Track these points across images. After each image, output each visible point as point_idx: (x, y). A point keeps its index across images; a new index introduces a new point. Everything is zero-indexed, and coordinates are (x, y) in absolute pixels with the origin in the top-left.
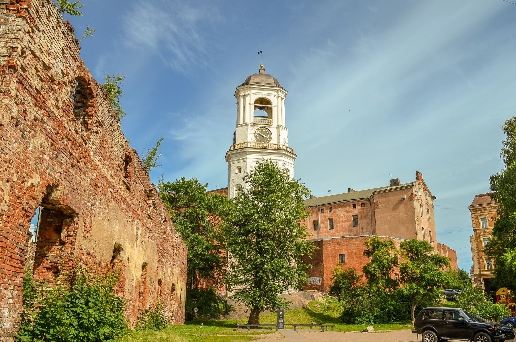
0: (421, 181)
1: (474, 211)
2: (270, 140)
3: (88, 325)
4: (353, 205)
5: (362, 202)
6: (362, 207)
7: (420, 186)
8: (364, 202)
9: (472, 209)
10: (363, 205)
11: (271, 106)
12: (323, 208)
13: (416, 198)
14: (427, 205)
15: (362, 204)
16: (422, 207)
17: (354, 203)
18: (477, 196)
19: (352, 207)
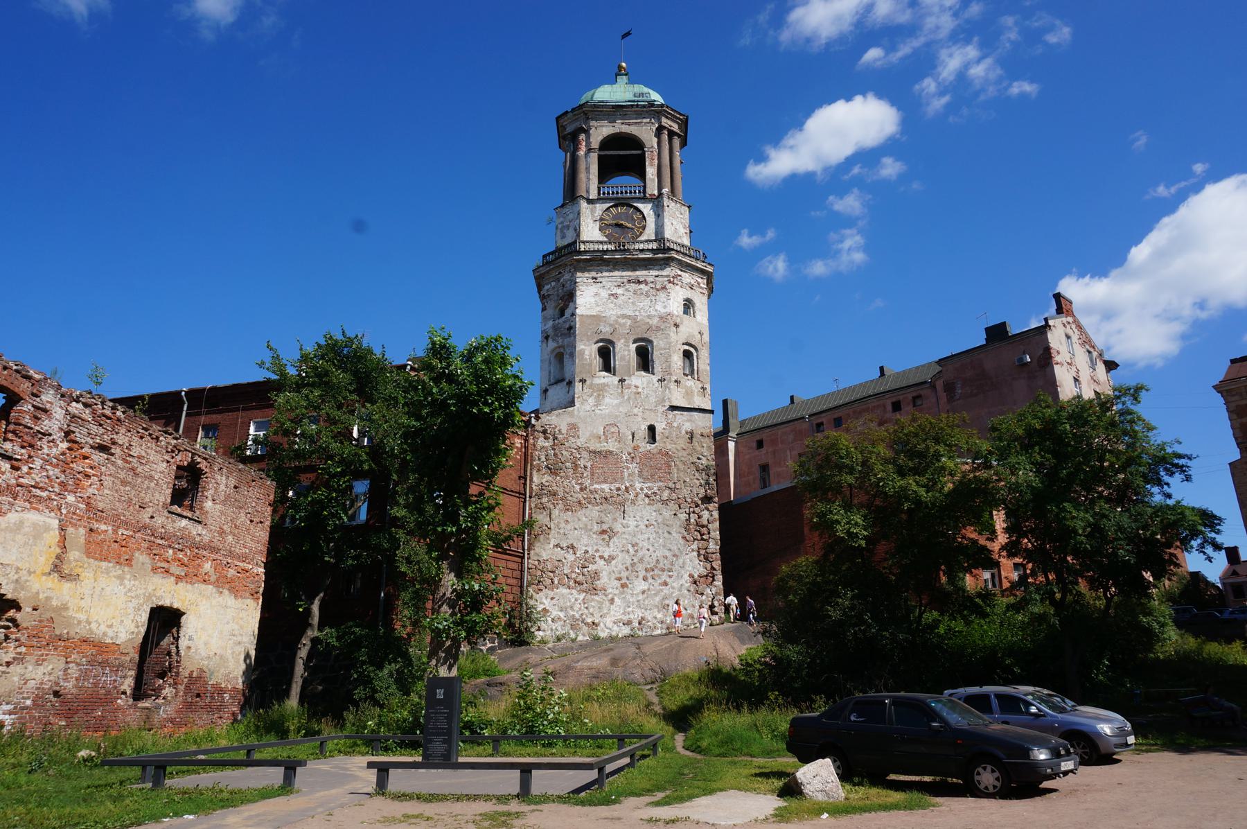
0: (1070, 319)
1: (1233, 395)
2: (641, 233)
3: (319, 722)
4: (893, 404)
5: (915, 394)
6: (914, 406)
7: (1070, 332)
8: (922, 393)
9: (1227, 391)
10: (919, 402)
11: (639, 152)
12: (820, 421)
13: (1057, 358)
14: (1095, 381)
15: (914, 398)
16: (1080, 384)
17: (894, 400)
18: (1233, 361)
19: (889, 408)
